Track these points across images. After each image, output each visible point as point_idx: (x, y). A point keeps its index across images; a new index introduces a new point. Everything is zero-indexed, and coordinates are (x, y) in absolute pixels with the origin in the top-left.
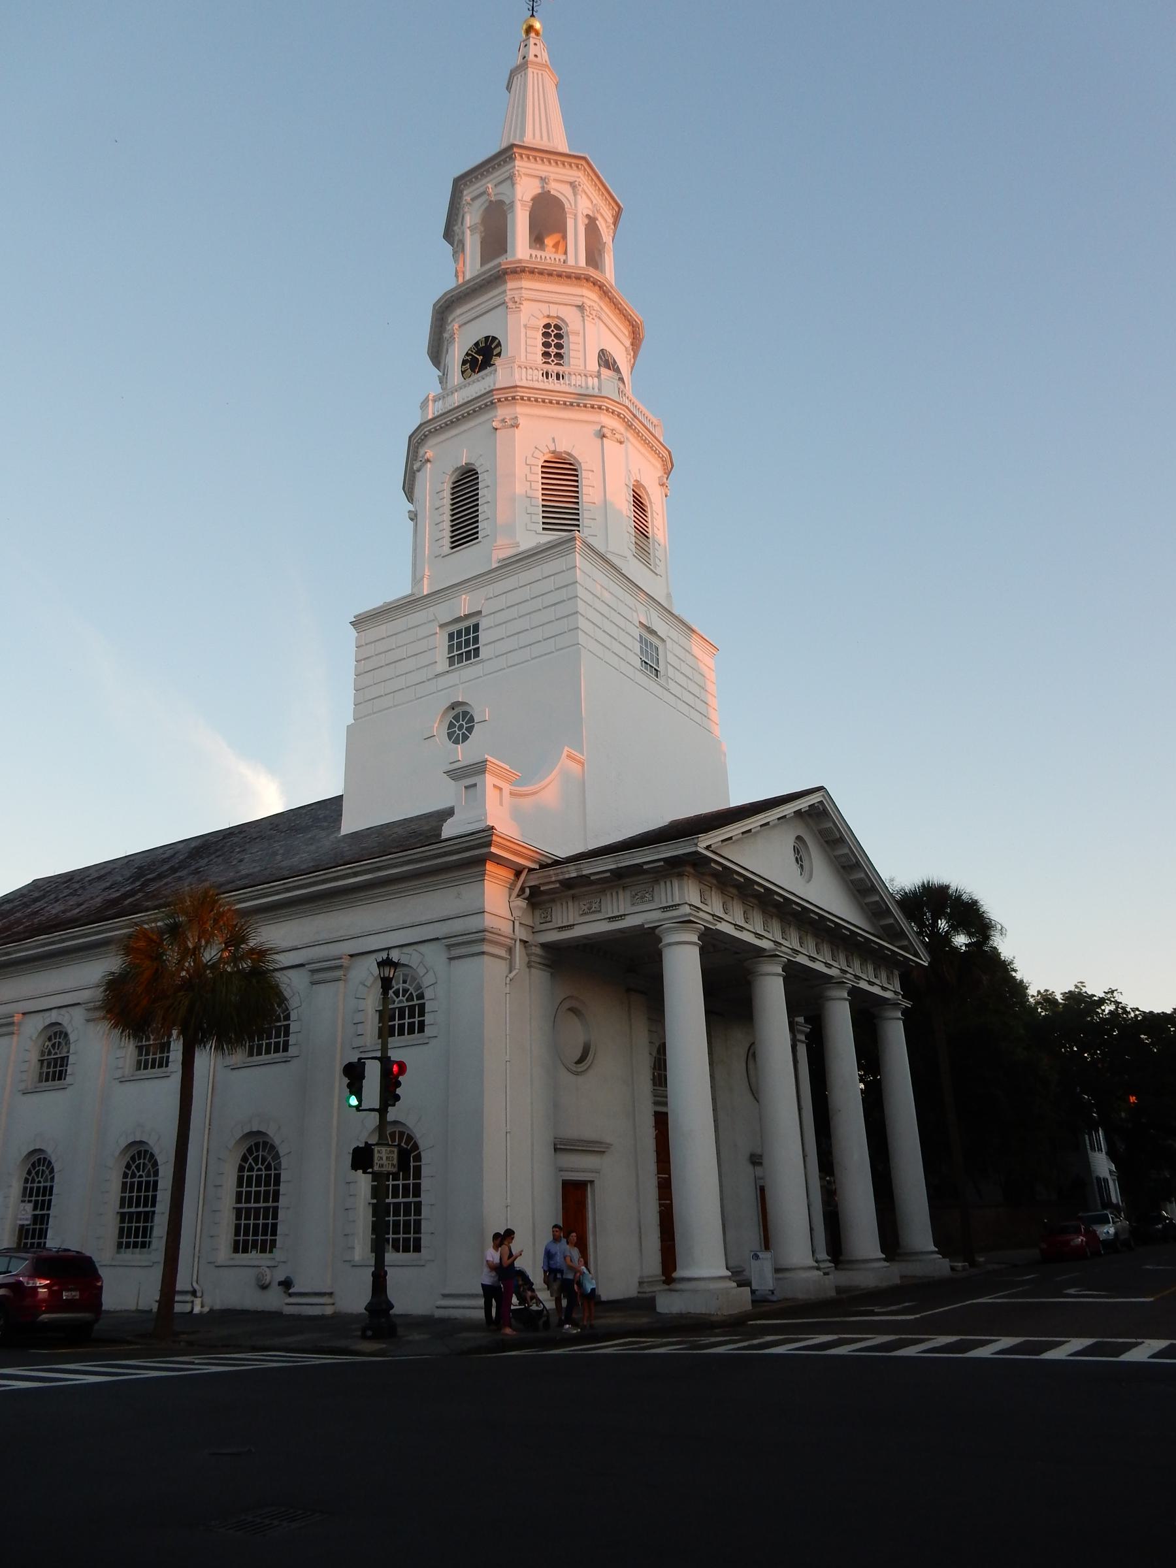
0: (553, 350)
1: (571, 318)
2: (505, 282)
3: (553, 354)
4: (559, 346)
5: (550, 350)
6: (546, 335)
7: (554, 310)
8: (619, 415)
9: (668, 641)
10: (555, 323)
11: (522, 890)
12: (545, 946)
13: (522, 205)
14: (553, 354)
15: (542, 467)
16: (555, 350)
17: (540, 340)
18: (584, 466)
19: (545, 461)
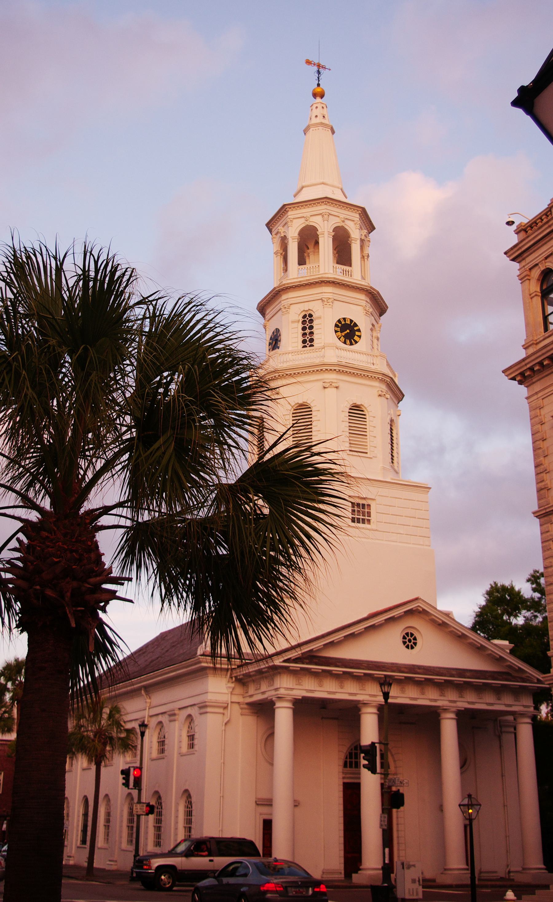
0: (308, 331)
1: (317, 309)
2: (281, 296)
3: (308, 333)
4: (311, 327)
5: (306, 331)
6: (304, 322)
7: (306, 306)
8: (335, 370)
9: (377, 498)
10: (309, 313)
11: (231, 678)
12: (248, 704)
13: (293, 239)
14: (308, 333)
15: (293, 413)
16: (309, 331)
17: (300, 326)
18: (313, 409)
19: (295, 410)
